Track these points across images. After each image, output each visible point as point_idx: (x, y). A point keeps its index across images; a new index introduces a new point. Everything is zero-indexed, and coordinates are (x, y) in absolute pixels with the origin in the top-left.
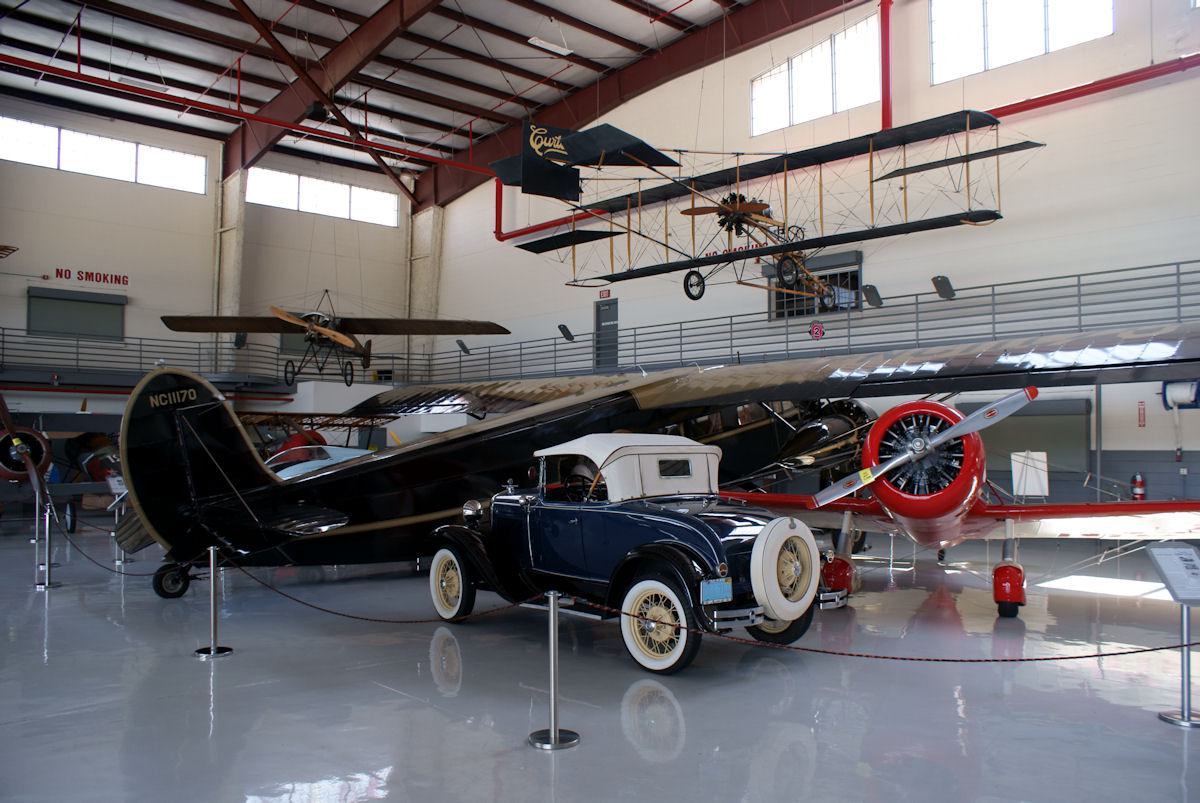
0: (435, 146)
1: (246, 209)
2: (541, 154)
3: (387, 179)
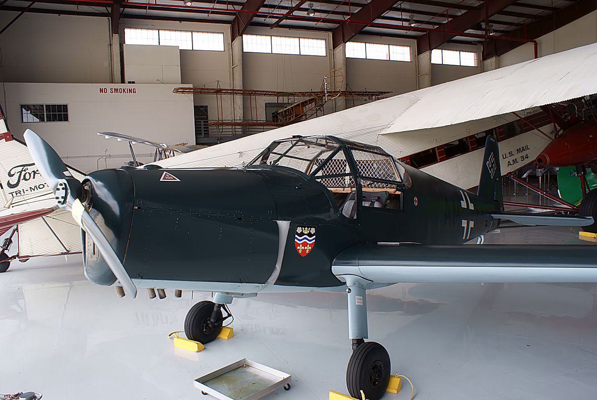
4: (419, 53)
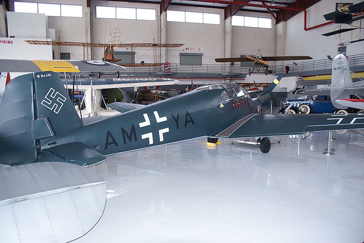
1: (232, 28)
2: (341, 12)
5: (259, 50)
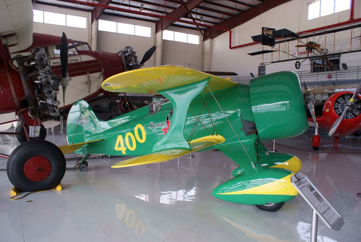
0: (211, 22)
3: (199, 32)
4: (157, 31)
5: (190, 64)
